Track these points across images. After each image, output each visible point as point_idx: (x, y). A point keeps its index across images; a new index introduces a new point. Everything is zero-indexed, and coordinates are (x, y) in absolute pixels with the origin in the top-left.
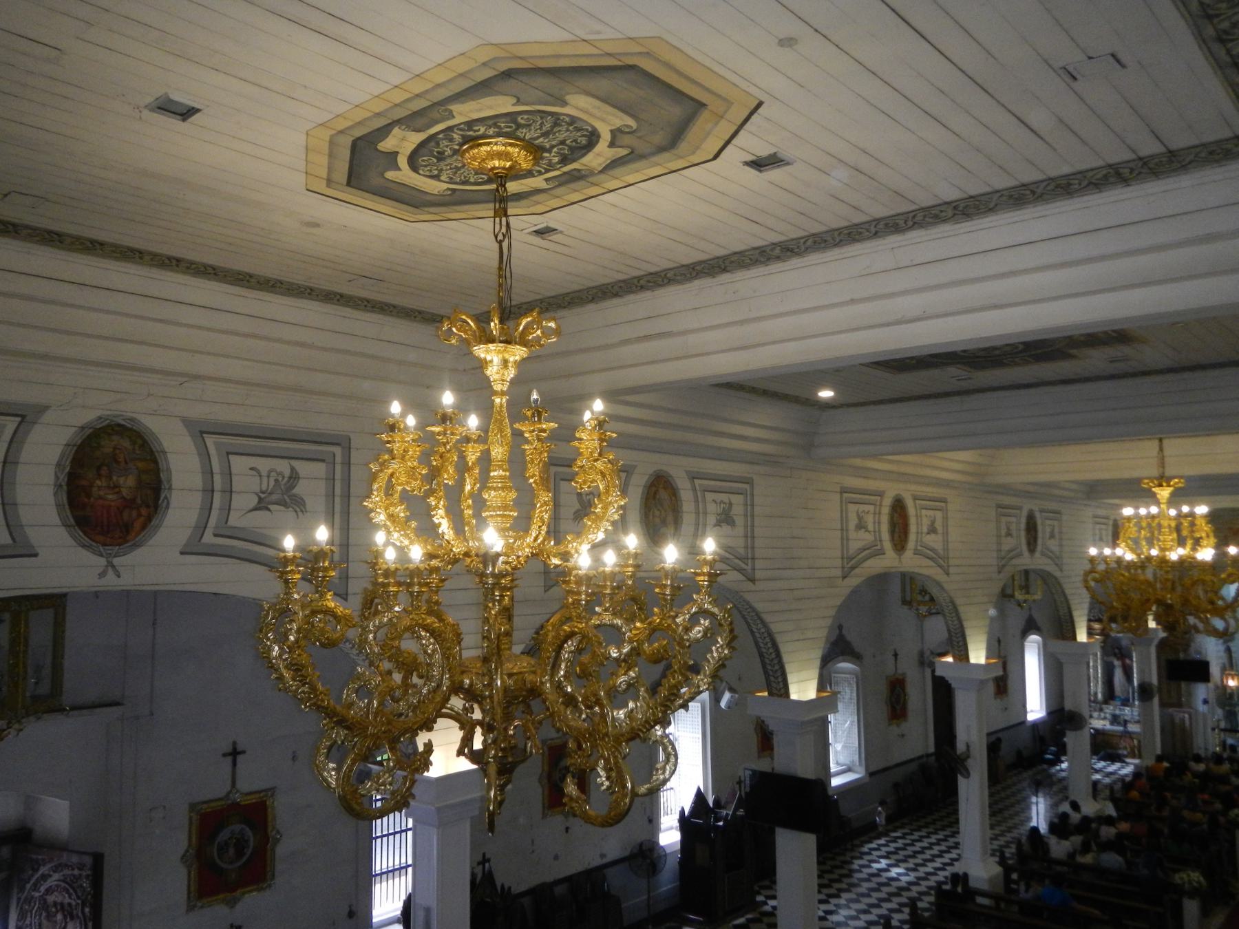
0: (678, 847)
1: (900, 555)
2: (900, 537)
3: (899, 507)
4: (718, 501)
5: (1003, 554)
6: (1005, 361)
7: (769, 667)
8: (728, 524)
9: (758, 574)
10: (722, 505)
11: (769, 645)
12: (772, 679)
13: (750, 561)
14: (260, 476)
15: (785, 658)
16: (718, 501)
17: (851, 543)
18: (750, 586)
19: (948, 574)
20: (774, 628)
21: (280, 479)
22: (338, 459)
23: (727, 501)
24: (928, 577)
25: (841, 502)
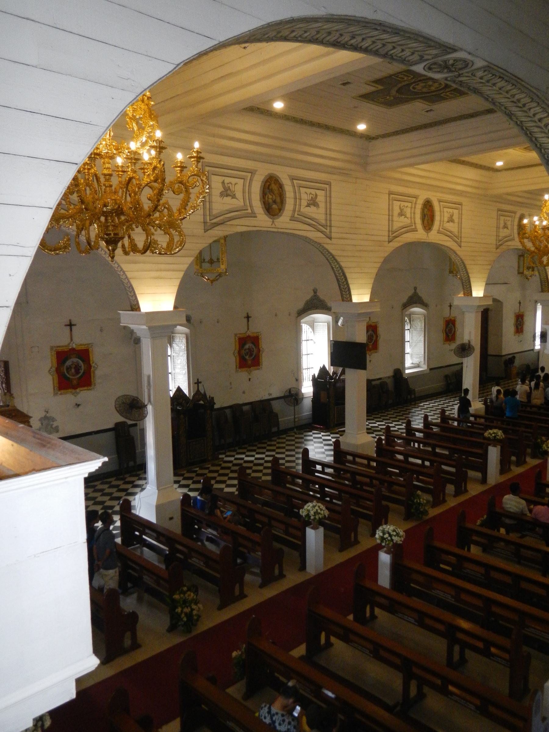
0: (312, 395)
2: (428, 222)
3: (428, 206)
4: (308, 193)
5: (500, 238)
6: (442, 95)
7: (342, 287)
8: (314, 206)
9: (333, 235)
10: (311, 196)
12: (344, 293)
13: (328, 228)
15: (350, 281)
16: (308, 193)
17: (395, 223)
18: (328, 241)
19: (460, 246)
20: (343, 264)
23: (314, 194)
24: (447, 247)
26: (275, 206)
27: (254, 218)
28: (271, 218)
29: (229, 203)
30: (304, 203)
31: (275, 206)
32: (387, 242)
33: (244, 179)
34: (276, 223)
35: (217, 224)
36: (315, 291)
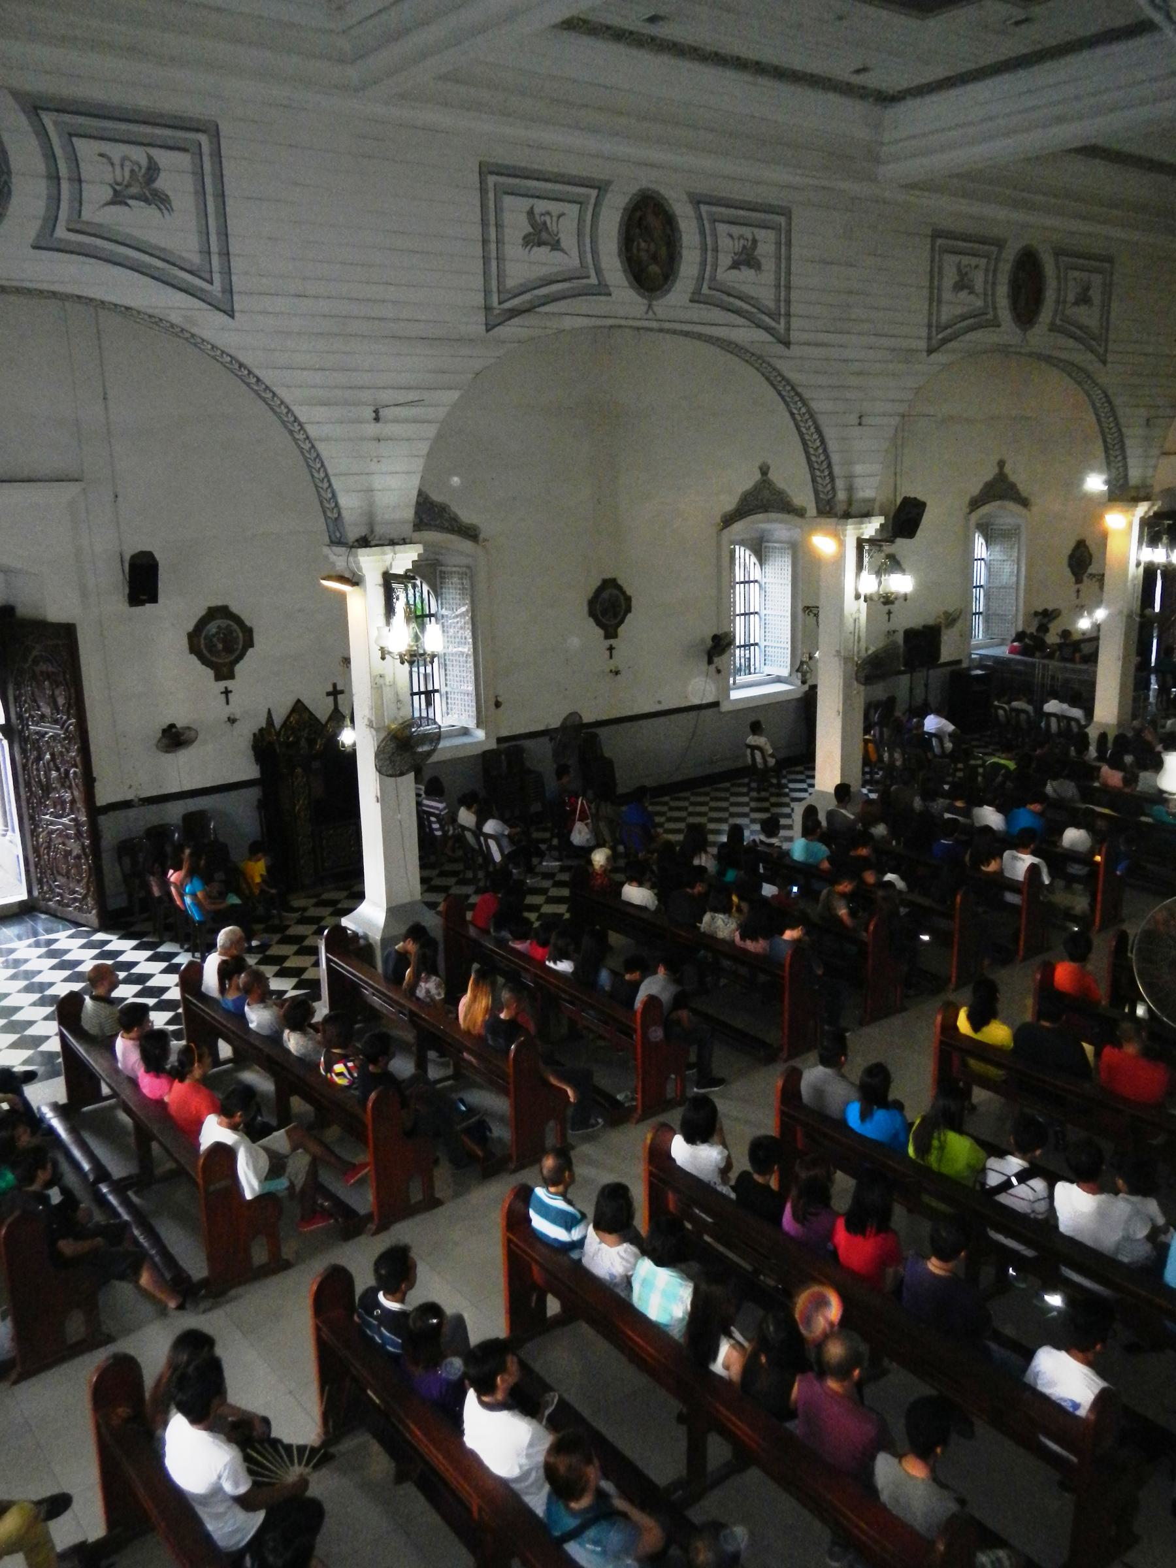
1: (1025, 330)
4: (736, 235)
7: (813, 459)
9: (795, 336)
10: (742, 242)
11: (812, 430)
12: (818, 473)
13: (782, 321)
14: (112, 164)
17: (944, 309)
18: (780, 349)
19: (1104, 362)
21: (136, 168)
22: (206, 149)
23: (750, 237)
25: (933, 249)
26: (654, 269)
27: (602, 298)
28: (644, 297)
29: (544, 261)
30: (725, 260)
31: (654, 269)
32: (925, 354)
33: (581, 203)
34: (655, 308)
35: (514, 313)
36: (765, 469)
